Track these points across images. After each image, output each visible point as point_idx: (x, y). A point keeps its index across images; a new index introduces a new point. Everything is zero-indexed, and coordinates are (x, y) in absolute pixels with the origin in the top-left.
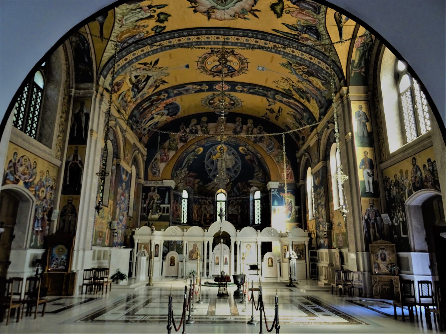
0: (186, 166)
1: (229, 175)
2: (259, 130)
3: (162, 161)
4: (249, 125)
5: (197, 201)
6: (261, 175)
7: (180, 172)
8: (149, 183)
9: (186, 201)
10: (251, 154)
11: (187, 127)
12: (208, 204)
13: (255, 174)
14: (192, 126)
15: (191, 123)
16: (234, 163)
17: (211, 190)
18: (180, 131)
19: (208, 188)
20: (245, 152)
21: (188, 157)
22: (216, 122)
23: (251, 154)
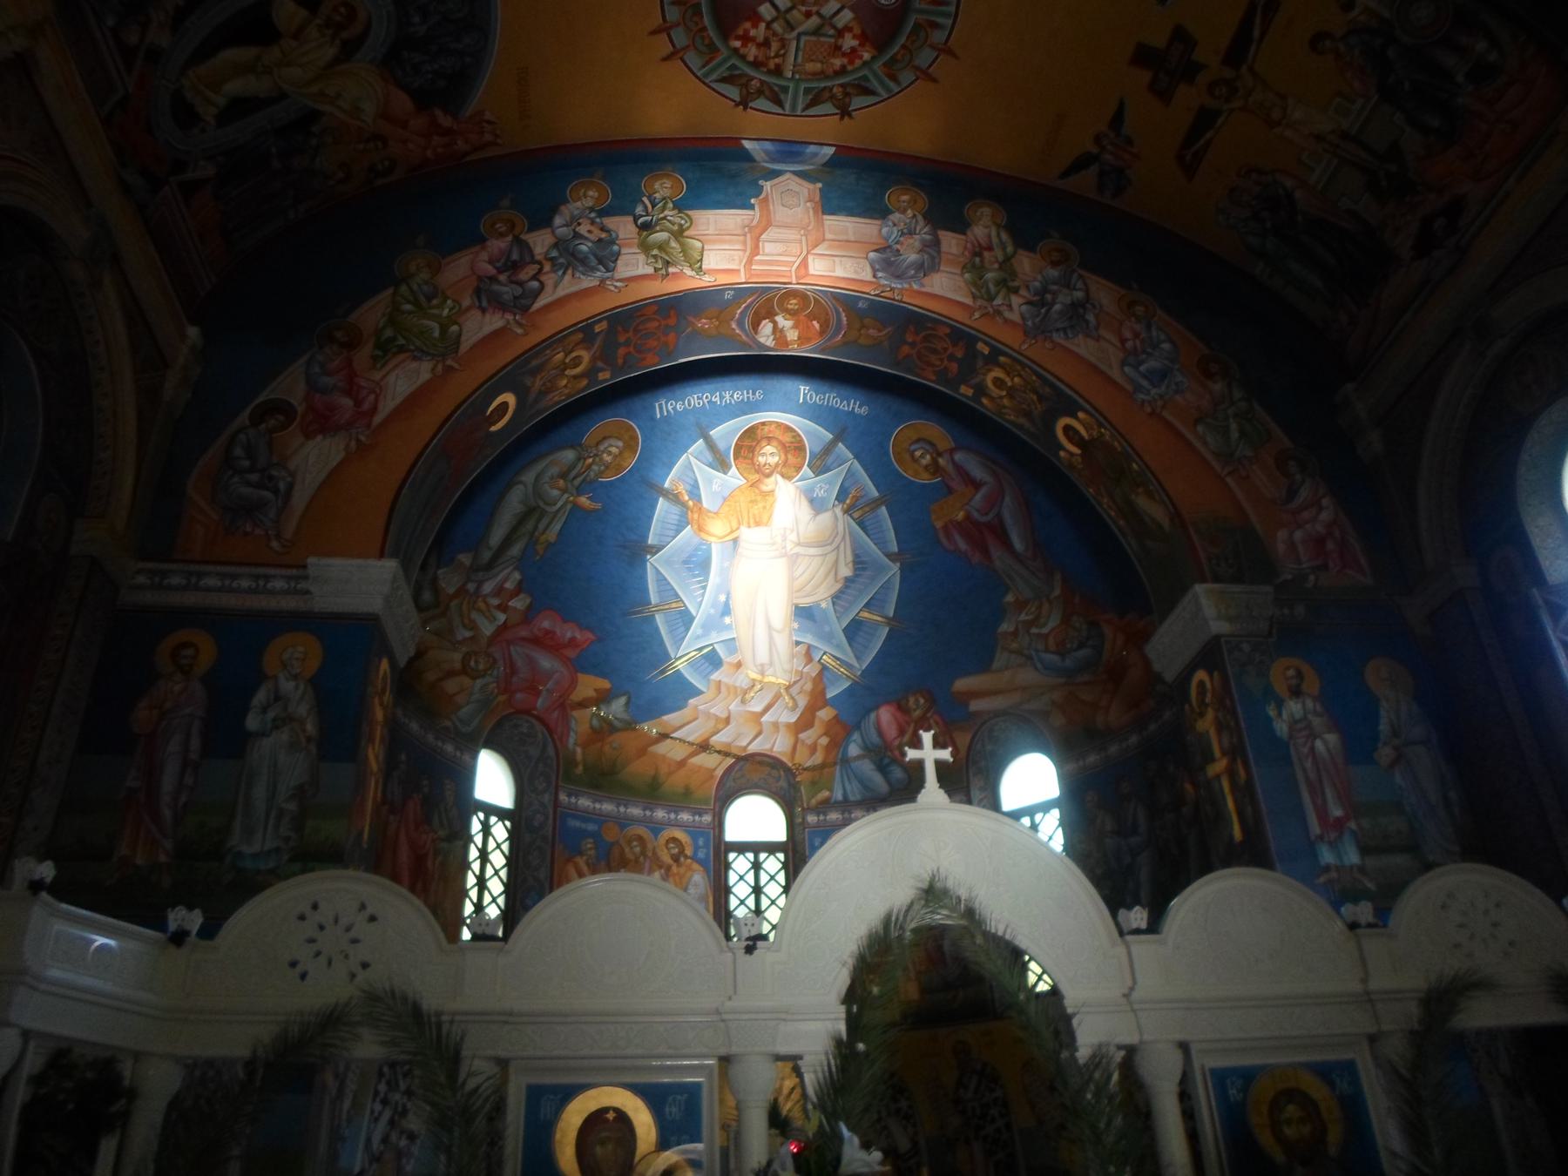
0: (515, 550)
1: (809, 657)
2: (1054, 264)
3: (321, 423)
4: (979, 232)
5: (585, 834)
6: (1054, 622)
7: (461, 591)
8: (176, 580)
9: (500, 831)
10: (978, 472)
11: (542, 220)
12: (667, 859)
13: (1005, 627)
14: (574, 221)
15: (566, 202)
16: (846, 571)
17: (682, 763)
18: (481, 240)
19: (662, 748)
20: (935, 469)
21: (529, 477)
22: (752, 207)
23: (978, 472)
